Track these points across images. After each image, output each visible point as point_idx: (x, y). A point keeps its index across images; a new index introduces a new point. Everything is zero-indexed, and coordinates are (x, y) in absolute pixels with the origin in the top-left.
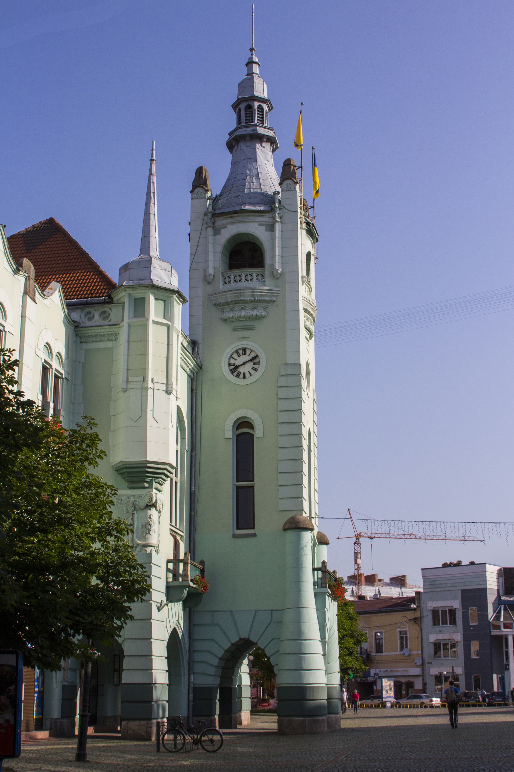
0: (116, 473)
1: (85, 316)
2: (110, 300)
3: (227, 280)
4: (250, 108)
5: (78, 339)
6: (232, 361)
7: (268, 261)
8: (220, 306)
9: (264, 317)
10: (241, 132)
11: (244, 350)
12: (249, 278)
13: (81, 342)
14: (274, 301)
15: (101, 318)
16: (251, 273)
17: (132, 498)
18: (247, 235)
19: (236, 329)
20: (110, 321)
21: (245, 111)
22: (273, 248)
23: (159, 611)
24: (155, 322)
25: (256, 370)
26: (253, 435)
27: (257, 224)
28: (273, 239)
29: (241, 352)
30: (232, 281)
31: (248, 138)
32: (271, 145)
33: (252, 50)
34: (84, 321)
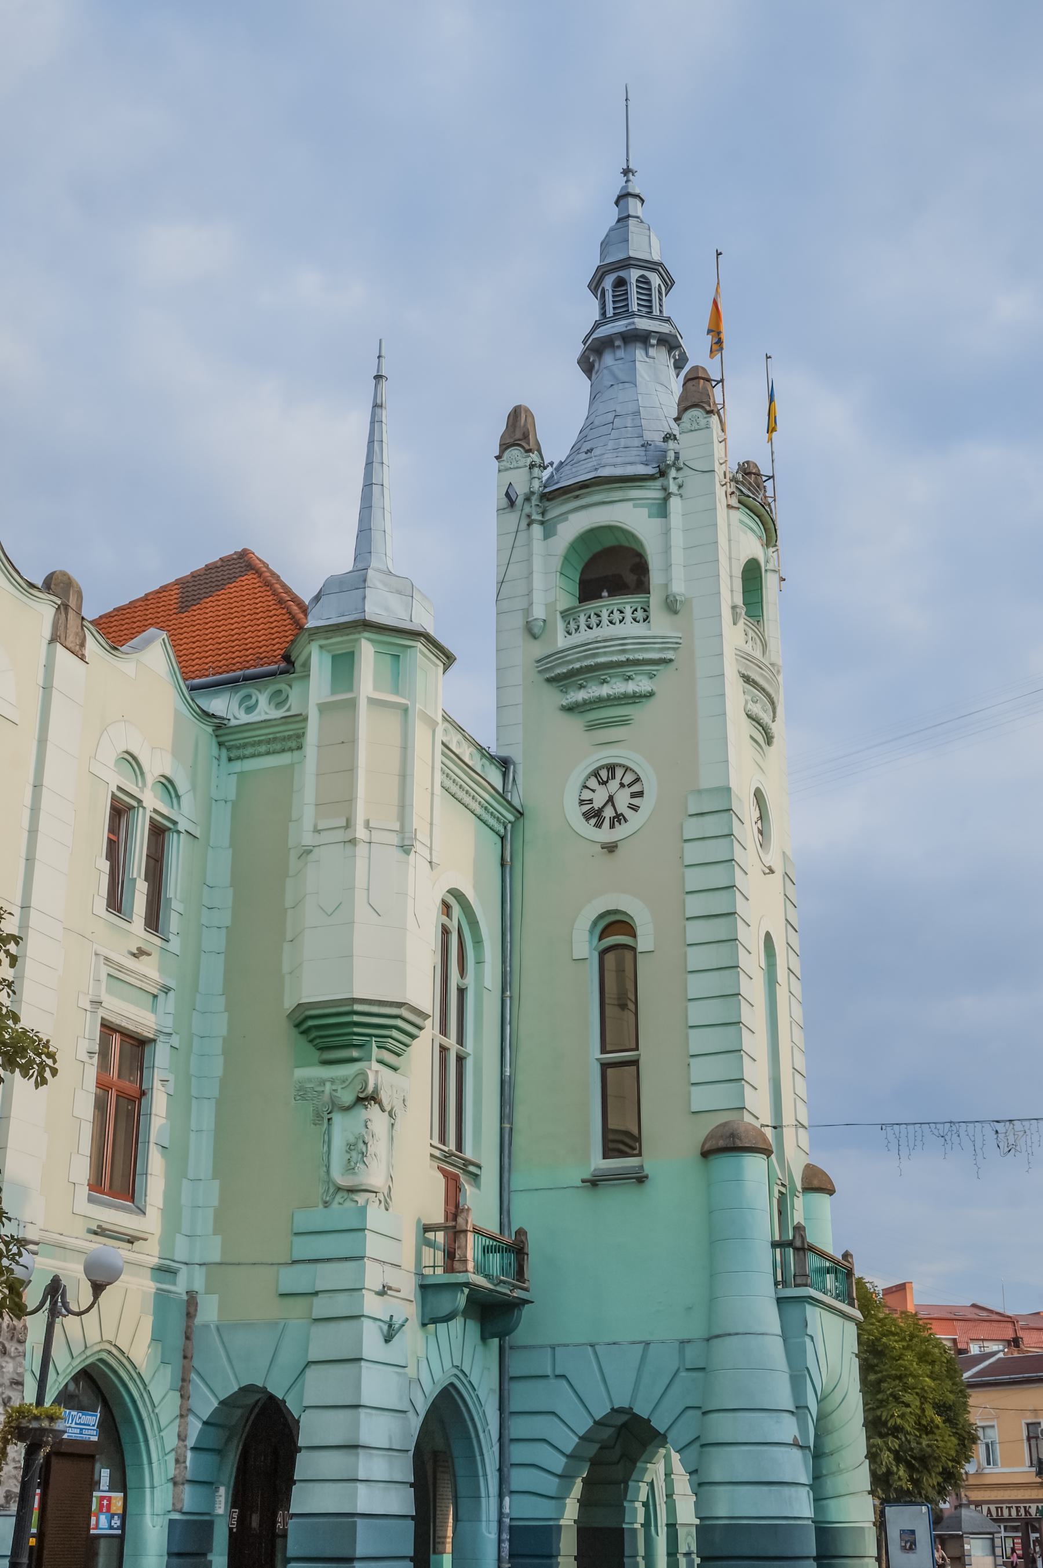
0: (294, 1032)
1: (240, 705)
2: (290, 667)
4: (621, 283)
5: (224, 752)
6: (587, 795)
7: (656, 578)
8: (561, 681)
10: (603, 332)
11: (611, 768)
13: (230, 760)
14: (671, 660)
15: (272, 706)
16: (621, 607)
17: (328, 1085)
18: (611, 529)
19: (592, 727)
20: (288, 710)
21: (613, 291)
22: (667, 550)
23: (387, 1341)
24: (371, 701)
25: (634, 808)
27: (630, 504)
28: (667, 532)
29: (604, 774)
30: (583, 627)
31: (617, 343)
32: (669, 352)
34: (238, 716)
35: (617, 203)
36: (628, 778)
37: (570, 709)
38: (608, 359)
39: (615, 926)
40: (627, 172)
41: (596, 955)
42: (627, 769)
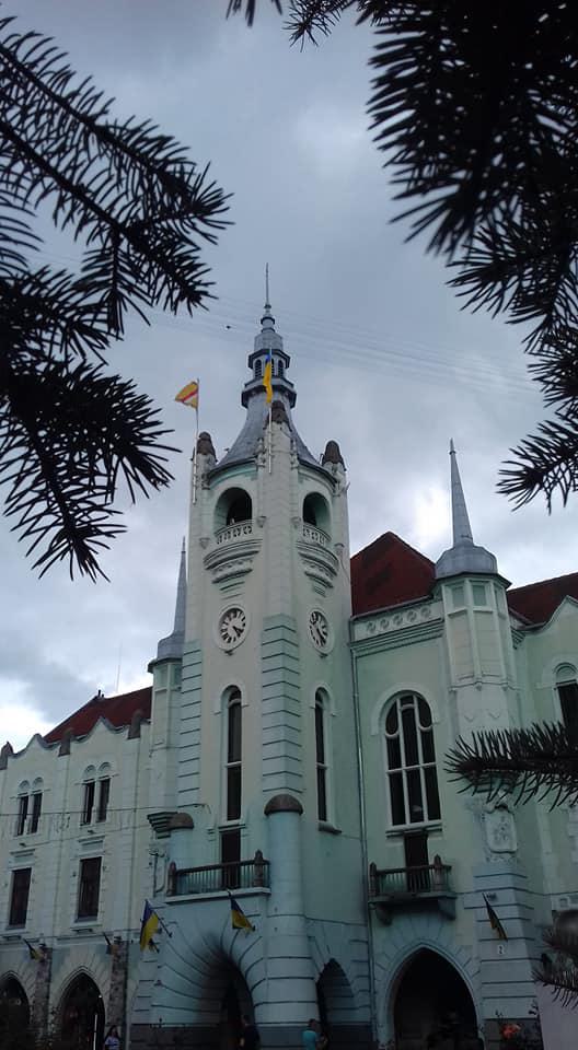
4: (259, 363)
6: (224, 627)
9: (250, 570)
10: (249, 387)
11: (235, 611)
12: (237, 532)
26: (239, 704)
29: (232, 615)
33: (268, 306)
35: (262, 321)
37: (218, 581)
38: (251, 401)
39: (234, 692)
40: (268, 306)
41: (226, 711)
42: (242, 612)
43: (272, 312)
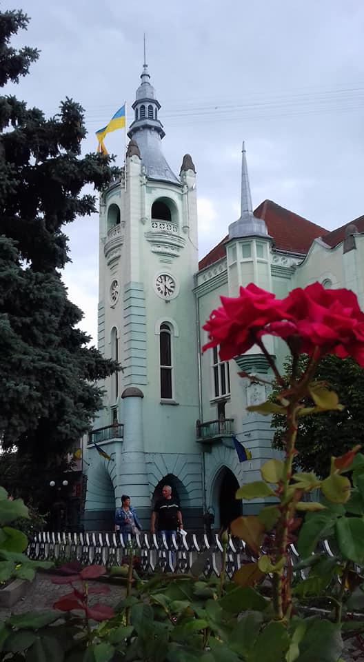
3: (155, 225)
11: (165, 276)
19: (162, 261)
26: (169, 335)
35: (141, 77)
36: (170, 281)
37: (153, 252)
40: (145, 66)
43: (149, 71)
